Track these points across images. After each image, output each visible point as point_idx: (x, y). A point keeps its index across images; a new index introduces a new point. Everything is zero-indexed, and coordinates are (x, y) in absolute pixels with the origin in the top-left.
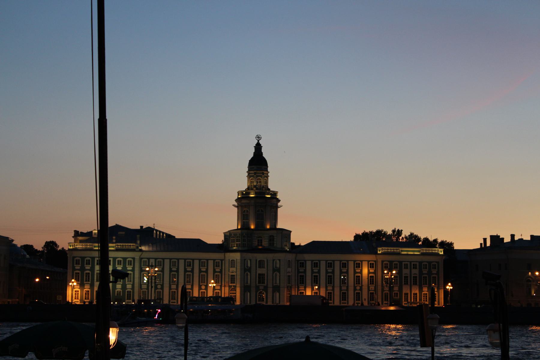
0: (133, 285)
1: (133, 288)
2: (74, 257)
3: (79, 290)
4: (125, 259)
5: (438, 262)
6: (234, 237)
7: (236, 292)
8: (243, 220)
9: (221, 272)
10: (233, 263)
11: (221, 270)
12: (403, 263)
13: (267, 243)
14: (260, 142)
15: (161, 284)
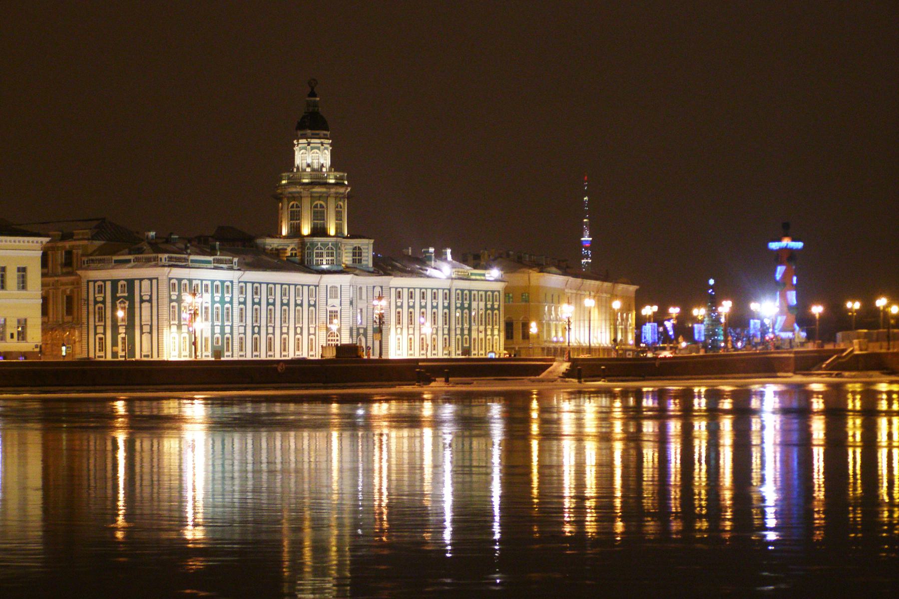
0: (232, 327)
1: (232, 333)
2: (170, 279)
3: (177, 336)
4: (223, 282)
5: (499, 292)
6: (321, 249)
7: (341, 338)
8: (314, 220)
9: (315, 306)
10: (333, 292)
11: (315, 302)
12: (473, 292)
13: (351, 259)
14: (315, 90)
15: (259, 325)
